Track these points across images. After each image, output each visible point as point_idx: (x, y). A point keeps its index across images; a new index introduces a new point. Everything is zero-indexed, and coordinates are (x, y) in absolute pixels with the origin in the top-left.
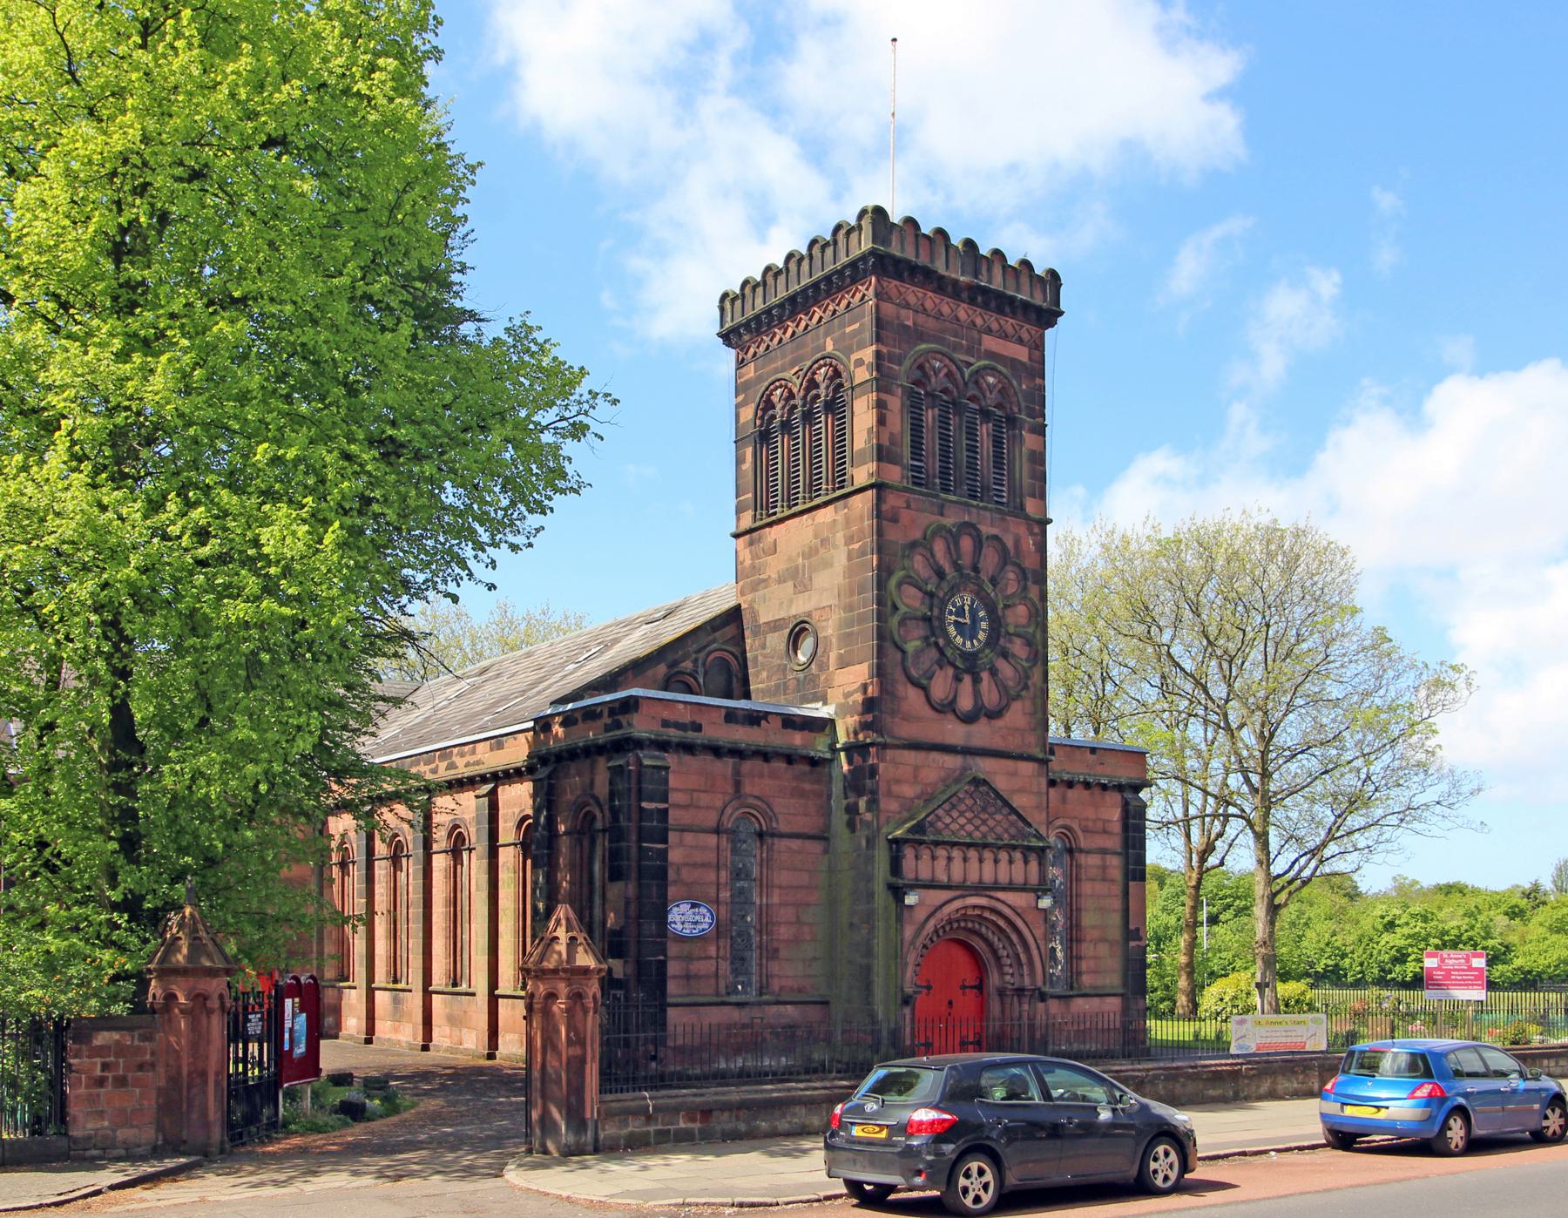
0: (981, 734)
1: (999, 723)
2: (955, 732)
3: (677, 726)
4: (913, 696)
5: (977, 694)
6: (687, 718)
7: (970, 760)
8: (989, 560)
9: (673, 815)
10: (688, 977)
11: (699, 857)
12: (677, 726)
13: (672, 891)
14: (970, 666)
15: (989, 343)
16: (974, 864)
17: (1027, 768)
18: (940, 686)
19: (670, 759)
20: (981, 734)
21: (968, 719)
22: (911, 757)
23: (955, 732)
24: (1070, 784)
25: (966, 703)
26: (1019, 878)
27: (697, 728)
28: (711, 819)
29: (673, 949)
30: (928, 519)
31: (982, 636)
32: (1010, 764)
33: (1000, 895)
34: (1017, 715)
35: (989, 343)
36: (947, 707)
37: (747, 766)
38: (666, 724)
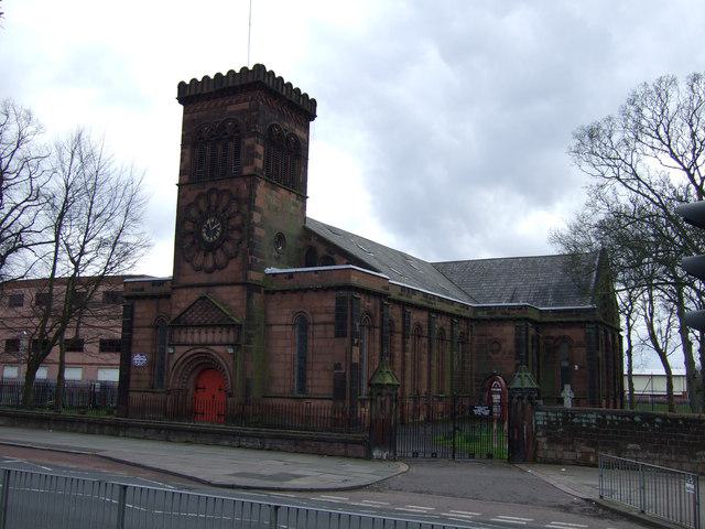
0: (216, 277)
1: (225, 270)
2: (203, 278)
3: (137, 290)
4: (188, 266)
5: (214, 259)
6: (141, 286)
7: (211, 289)
8: (225, 199)
9: (136, 323)
10: (138, 381)
11: (144, 336)
12: (137, 290)
13: (133, 350)
14: (211, 248)
15: (231, 108)
16: (196, 335)
17: (237, 289)
18: (199, 260)
19: (137, 303)
20: (216, 277)
21: (210, 271)
22: (185, 291)
23: (203, 278)
24: (306, 290)
25: (210, 264)
26: (224, 340)
27: (143, 289)
28: (148, 323)
29: (133, 371)
30: (196, 192)
31: (218, 234)
32: (229, 288)
33: (212, 347)
34: (233, 266)
35: (231, 108)
36: (198, 269)
37: (161, 301)
38: (133, 290)
